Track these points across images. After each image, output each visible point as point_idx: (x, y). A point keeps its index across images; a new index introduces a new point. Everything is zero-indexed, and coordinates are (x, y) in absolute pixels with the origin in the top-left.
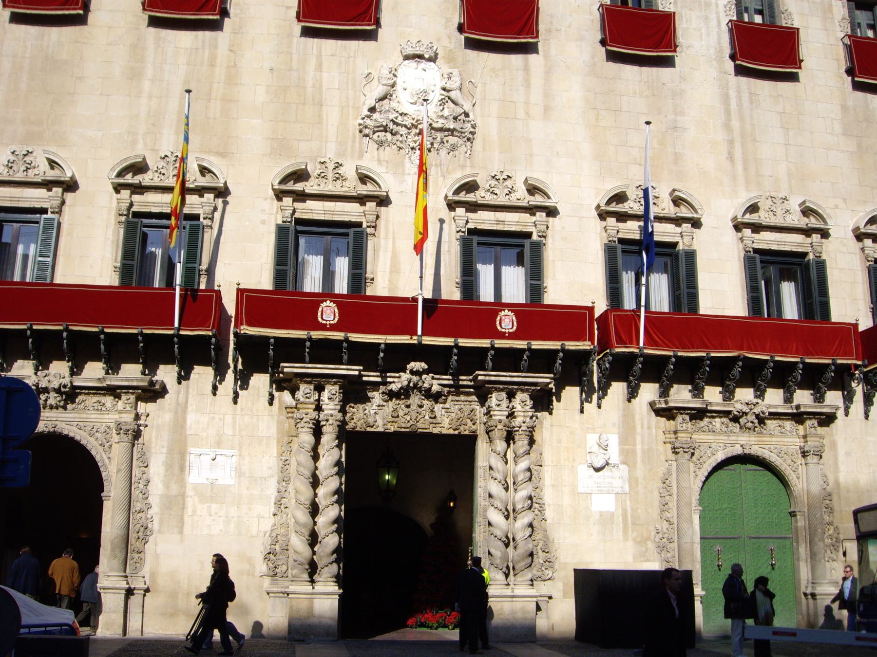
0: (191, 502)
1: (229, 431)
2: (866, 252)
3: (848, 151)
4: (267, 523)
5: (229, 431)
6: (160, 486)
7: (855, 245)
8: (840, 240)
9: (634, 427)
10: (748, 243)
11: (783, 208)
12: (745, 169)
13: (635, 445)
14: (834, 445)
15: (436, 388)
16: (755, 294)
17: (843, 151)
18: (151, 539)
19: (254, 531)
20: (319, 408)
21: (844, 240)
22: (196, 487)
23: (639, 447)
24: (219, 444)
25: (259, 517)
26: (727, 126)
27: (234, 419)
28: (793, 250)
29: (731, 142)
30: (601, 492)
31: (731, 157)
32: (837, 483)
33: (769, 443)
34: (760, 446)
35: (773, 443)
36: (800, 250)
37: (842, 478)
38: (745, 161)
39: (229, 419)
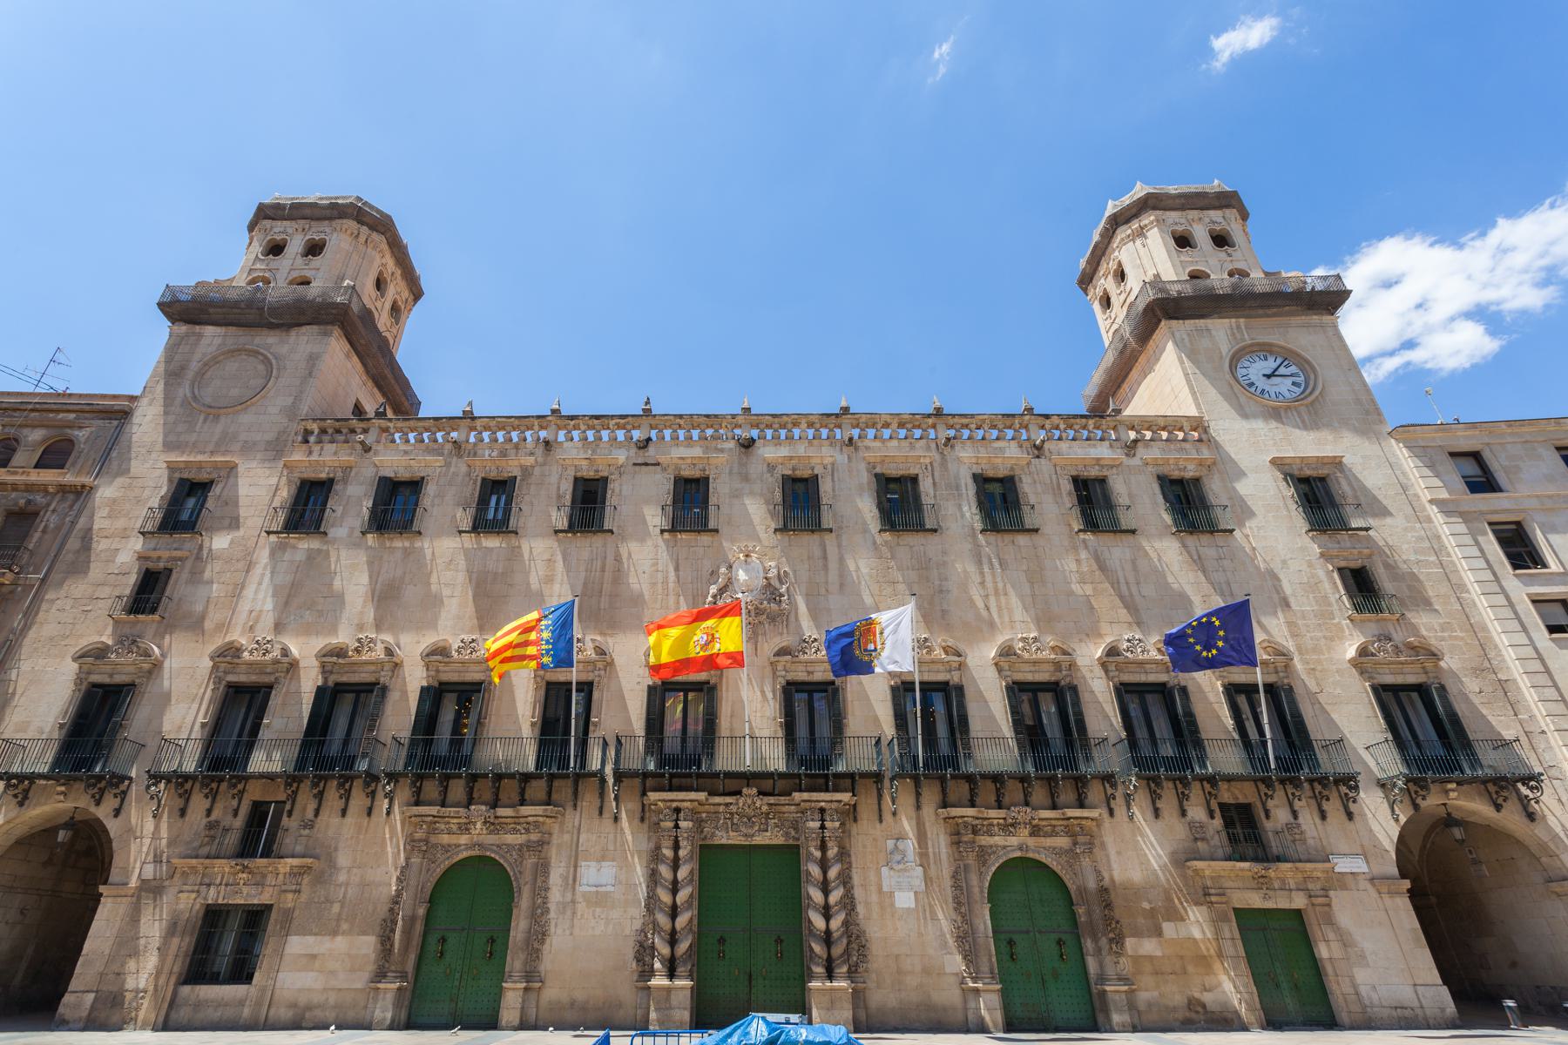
1: (611, 847)
4: (638, 925)
5: (611, 847)
6: (558, 894)
9: (925, 833)
13: (927, 849)
14: (1103, 846)
15: (765, 808)
18: (548, 941)
19: (627, 932)
20: (677, 826)
22: (584, 894)
23: (930, 850)
24: (603, 858)
25: (632, 918)
27: (616, 837)
32: (1112, 880)
39: (611, 836)
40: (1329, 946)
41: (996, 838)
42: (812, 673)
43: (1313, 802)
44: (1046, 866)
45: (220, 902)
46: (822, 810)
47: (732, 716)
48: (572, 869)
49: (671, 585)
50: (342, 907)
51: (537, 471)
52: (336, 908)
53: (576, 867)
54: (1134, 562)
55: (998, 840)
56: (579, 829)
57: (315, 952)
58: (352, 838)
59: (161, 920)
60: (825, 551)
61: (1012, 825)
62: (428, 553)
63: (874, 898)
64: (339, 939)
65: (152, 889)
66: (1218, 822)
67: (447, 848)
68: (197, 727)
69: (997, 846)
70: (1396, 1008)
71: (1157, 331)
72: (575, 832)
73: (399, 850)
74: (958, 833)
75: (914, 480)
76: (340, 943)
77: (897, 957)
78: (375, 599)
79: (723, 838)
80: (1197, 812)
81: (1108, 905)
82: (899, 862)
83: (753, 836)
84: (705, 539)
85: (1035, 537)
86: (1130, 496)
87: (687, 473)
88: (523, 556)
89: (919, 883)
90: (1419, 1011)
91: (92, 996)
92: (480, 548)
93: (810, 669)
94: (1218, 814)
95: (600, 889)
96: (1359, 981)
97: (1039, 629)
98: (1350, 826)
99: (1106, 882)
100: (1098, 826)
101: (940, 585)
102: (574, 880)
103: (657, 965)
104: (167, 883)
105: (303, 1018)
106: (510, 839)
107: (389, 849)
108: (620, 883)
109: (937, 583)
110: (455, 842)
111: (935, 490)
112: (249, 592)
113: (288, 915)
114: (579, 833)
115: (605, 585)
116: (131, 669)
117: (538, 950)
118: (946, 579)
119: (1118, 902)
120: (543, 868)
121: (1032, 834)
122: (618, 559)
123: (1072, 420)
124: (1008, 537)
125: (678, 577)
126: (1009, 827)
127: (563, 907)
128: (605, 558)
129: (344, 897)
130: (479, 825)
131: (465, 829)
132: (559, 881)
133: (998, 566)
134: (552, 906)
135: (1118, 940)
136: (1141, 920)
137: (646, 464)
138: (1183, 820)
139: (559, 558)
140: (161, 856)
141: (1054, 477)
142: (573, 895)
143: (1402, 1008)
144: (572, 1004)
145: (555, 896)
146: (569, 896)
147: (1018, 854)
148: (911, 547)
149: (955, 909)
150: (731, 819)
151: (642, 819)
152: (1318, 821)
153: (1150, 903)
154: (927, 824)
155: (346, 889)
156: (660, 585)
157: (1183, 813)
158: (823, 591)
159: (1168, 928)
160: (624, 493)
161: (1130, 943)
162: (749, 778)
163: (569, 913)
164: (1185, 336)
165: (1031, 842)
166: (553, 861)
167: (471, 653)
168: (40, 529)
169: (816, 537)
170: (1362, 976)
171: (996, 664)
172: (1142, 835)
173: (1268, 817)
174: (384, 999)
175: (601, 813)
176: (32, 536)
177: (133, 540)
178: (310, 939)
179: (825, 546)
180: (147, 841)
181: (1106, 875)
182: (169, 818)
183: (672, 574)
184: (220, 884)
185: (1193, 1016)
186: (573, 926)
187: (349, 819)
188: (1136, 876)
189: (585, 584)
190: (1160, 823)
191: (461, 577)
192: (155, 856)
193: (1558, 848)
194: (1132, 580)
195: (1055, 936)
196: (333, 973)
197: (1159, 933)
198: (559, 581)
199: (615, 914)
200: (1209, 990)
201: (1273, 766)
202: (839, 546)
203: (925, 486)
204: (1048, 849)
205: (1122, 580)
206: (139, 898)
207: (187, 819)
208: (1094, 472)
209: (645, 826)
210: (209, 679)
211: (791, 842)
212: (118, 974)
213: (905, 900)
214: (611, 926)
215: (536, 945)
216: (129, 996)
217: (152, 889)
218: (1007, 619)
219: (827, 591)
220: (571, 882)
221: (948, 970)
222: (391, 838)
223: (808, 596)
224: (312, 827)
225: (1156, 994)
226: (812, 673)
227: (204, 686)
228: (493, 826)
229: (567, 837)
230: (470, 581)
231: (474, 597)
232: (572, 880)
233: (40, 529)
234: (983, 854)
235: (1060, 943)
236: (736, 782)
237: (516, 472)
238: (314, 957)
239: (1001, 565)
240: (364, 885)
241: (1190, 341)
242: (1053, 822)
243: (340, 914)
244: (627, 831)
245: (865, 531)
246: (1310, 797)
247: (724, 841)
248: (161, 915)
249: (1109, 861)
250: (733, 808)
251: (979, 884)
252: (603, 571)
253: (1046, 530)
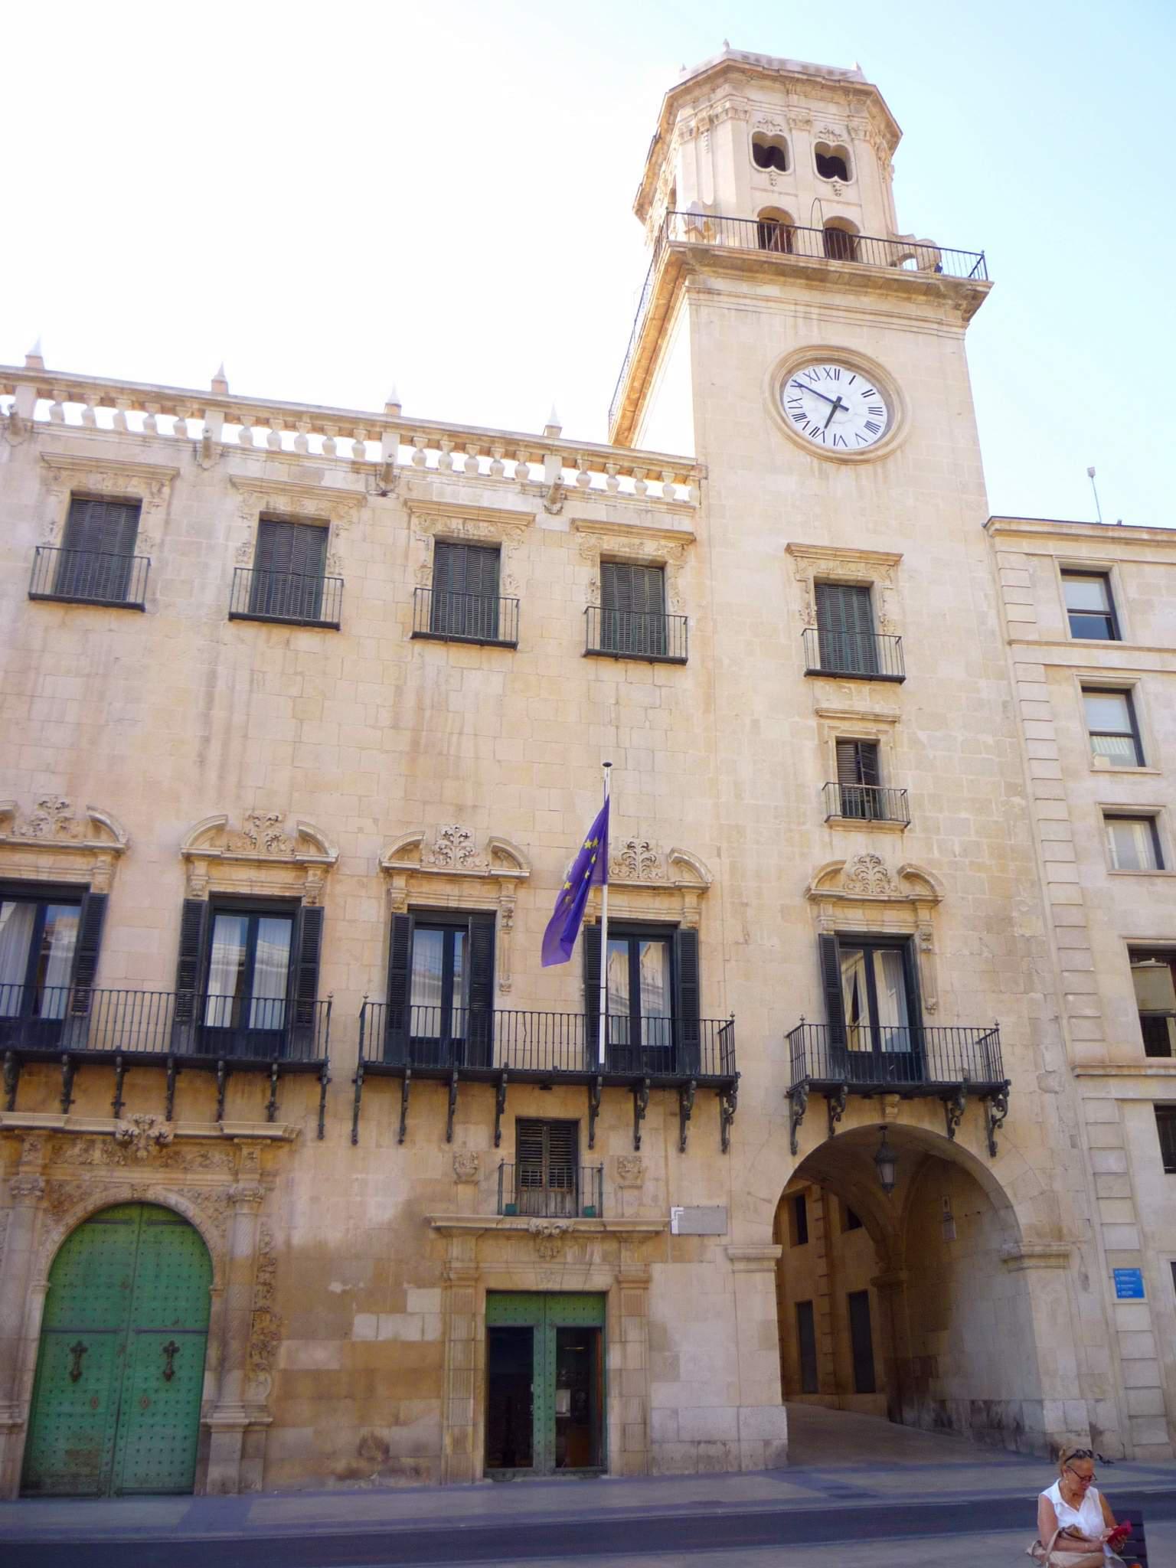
2: (393, 895)
3: (394, 751)
7: (377, 887)
8: (356, 878)
10: (198, 883)
11: (270, 832)
12: (221, 778)
14: (290, 1185)
16: (189, 959)
17: (387, 752)
21: (365, 880)
26: (206, 718)
28: (276, 894)
29: (206, 740)
31: (202, 760)
32: (288, 1243)
33: (181, 1182)
34: (165, 1186)
35: (188, 1183)
36: (287, 894)
38: (223, 767)
40: (624, 1351)
43: (676, 1121)
66: (507, 1151)
70: (699, 1443)
80: (474, 1136)
90: (733, 1447)
94: (509, 1133)
96: (655, 1403)
98: (722, 1161)
138: (446, 1147)
143: (709, 1442)
152: (672, 1151)
153: (344, 1282)
157: (449, 1138)
159: (365, 1326)
170: (662, 1395)
173: (591, 1147)
181: (279, 1238)
185: (363, 1464)
188: (334, 1235)
190: (402, 1150)
193: (1015, 1195)
197: (344, 1331)
200: (405, 1424)
201: (602, 1060)
225: (308, 1432)
235: (171, 1351)
246: (673, 1114)
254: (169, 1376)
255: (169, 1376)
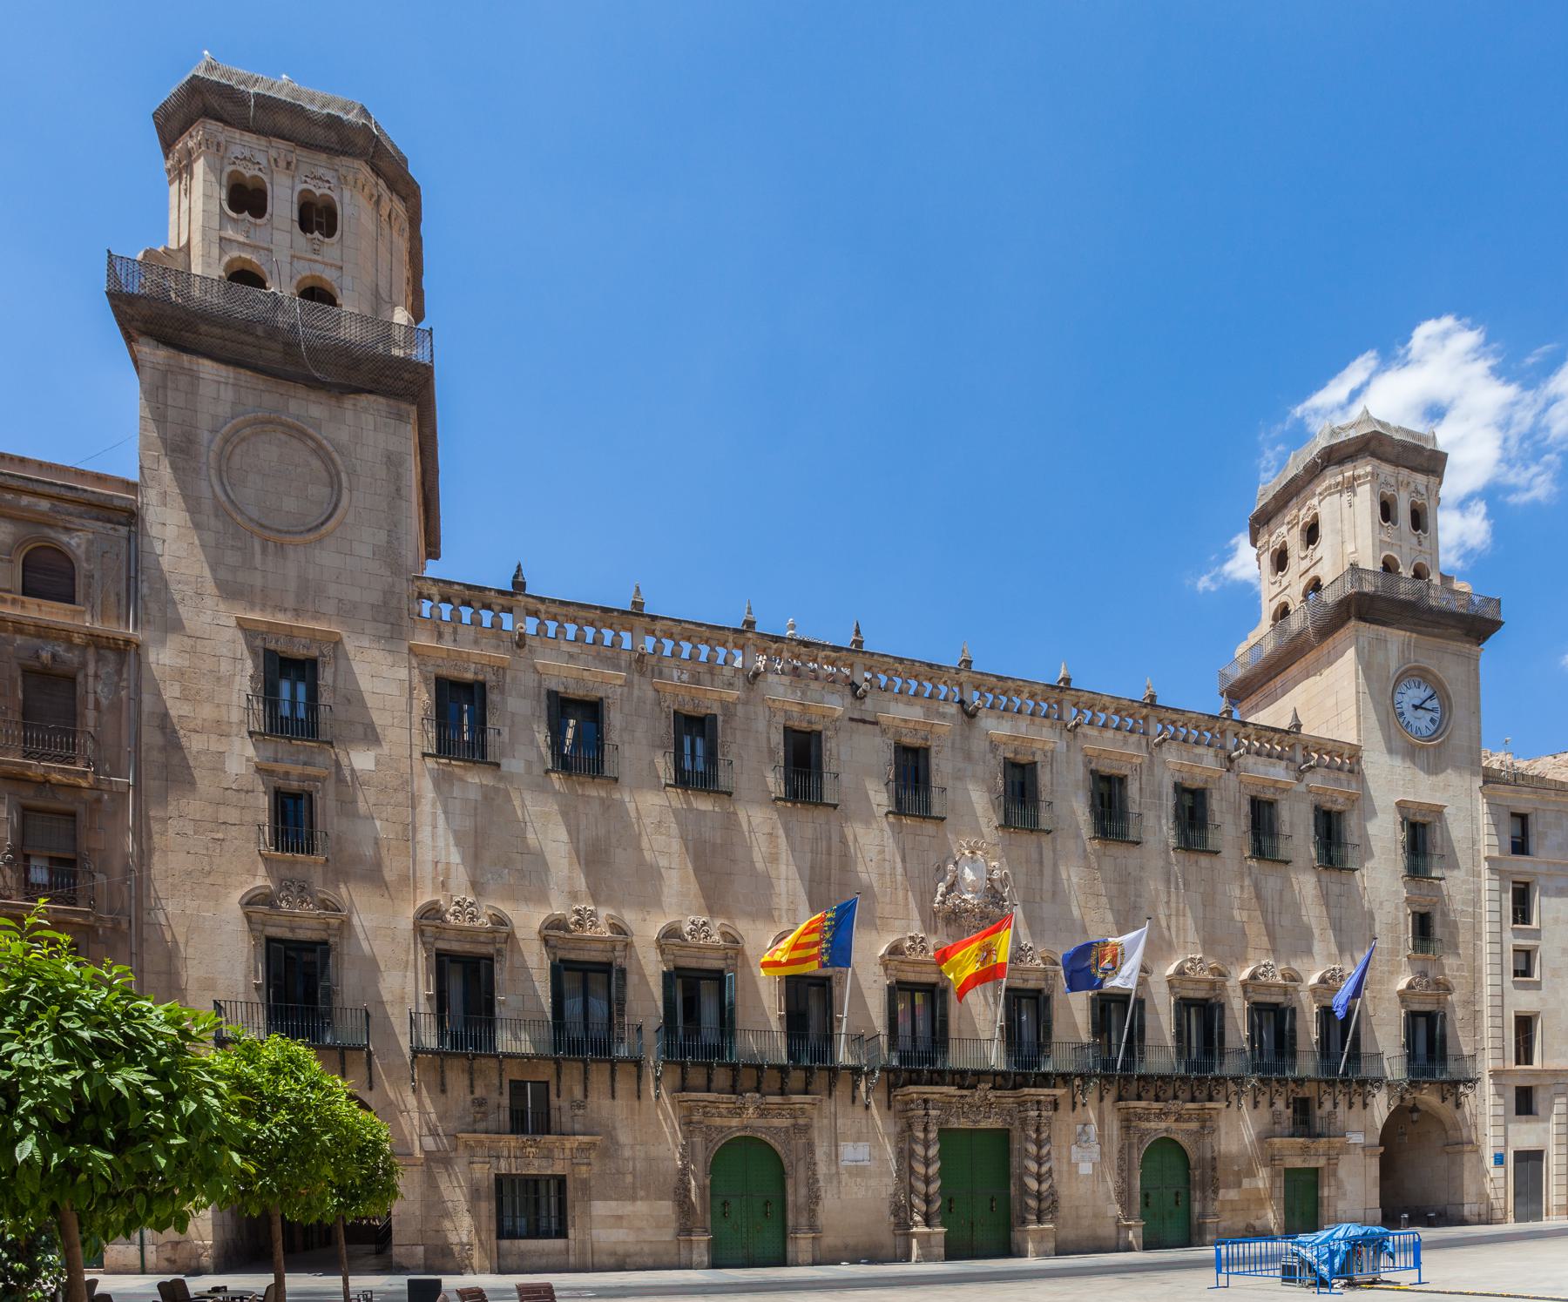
0: (845, 1177)
1: (865, 1130)
4: (891, 1190)
5: (865, 1130)
6: (824, 1168)
18: (821, 1203)
19: (883, 1196)
24: (858, 1139)
30: (1084, 1161)
32: (1219, 1151)
37: (1223, 1148)
39: (864, 1121)
41: (1152, 1123)
42: (1027, 980)
44: (1177, 1143)
45: (514, 1172)
46: (1039, 1102)
47: (959, 1018)
48: (833, 1148)
49: (899, 878)
50: (634, 1177)
51: (740, 710)
52: (629, 1179)
53: (836, 1146)
54: (1281, 892)
55: (1153, 1125)
56: (836, 1115)
57: (620, 1213)
58: (627, 1118)
59: (460, 1187)
60: (1041, 854)
61: (1164, 1114)
62: (631, 807)
63: (1065, 1167)
64: (639, 1203)
65: (437, 1161)
67: (720, 1129)
68: (422, 1000)
69: (1151, 1129)
71: (1342, 630)
72: (832, 1117)
73: (675, 1131)
74: (1128, 1120)
75: (1122, 780)
76: (641, 1207)
77: (1077, 1207)
78: (582, 862)
79: (955, 1123)
81: (1214, 1169)
82: (1086, 1142)
83: (979, 1121)
84: (929, 827)
85: (1214, 859)
86: (1292, 825)
87: (908, 740)
88: (741, 826)
89: (1096, 1156)
91: (422, 1247)
92: (691, 809)
93: (1025, 977)
95: (858, 1163)
97: (1204, 952)
99: (1216, 1154)
100: (1218, 1114)
101: (1135, 901)
102: (837, 1156)
103: (917, 1218)
104: (452, 1155)
105: (625, 1263)
106: (777, 1122)
107: (666, 1129)
108: (875, 1158)
109: (1133, 899)
110: (727, 1124)
111: (1141, 798)
112: (424, 834)
113: (585, 1185)
114: (836, 1119)
115: (833, 871)
116: (314, 923)
117: (814, 1210)
118: (1140, 896)
119: (1220, 1166)
120: (810, 1148)
121: (1176, 1120)
122: (843, 841)
123: (1263, 732)
124: (1193, 857)
125: (905, 869)
126: (1162, 1115)
127: (829, 1178)
128: (830, 838)
129: (634, 1169)
130: (751, 1110)
131: (738, 1111)
132: (824, 1158)
133: (1182, 887)
134: (821, 1177)
135: (1216, 1192)
136: (1231, 1178)
137: (864, 721)
139: (781, 832)
140: (437, 1130)
141: (1237, 794)
142: (837, 1167)
144: (846, 1247)
145: (822, 1169)
146: (833, 1170)
147: (1164, 1135)
148: (1115, 859)
149: (1118, 1174)
150: (963, 1108)
151: (889, 1107)
154: (1106, 1113)
155: (634, 1163)
156: (888, 876)
158: (1038, 899)
159: (1246, 1183)
160: (843, 757)
161: (1222, 1192)
162: (980, 1075)
163: (835, 1182)
164: (1366, 645)
165: (1174, 1126)
166: (816, 1141)
167: (706, 937)
168: (91, 705)
169: (1034, 837)
171: (1169, 981)
172: (1244, 1121)
174: (698, 1247)
175: (853, 1102)
176: (84, 716)
177: (237, 742)
178: (613, 1204)
179: (1041, 848)
180: (415, 1115)
181: (1216, 1148)
182: (428, 1092)
183: (899, 865)
184: (509, 1157)
186: (839, 1192)
187: (619, 1102)
189: (812, 868)
191: (676, 845)
192: (429, 1129)
194: (1277, 911)
195: (1174, 1190)
196: (640, 1229)
197: (1239, 1185)
198: (785, 862)
199: (873, 1183)
202: (1054, 850)
203: (1133, 789)
204: (1181, 1131)
205: (1270, 910)
206: (429, 1168)
207: (449, 1094)
208: (1268, 795)
209: (892, 1113)
210: (415, 944)
211: (1007, 1127)
212: (438, 1231)
213: (1085, 1169)
214: (870, 1192)
215: (812, 1207)
216: (456, 1249)
217: (437, 1161)
218: (1182, 940)
219: (1041, 898)
220: (833, 1158)
221: (1109, 1214)
222: (665, 1120)
223: (1025, 902)
224: (584, 1107)
226: (1027, 980)
227: (412, 952)
228: (763, 1112)
229: (826, 1121)
230: (687, 850)
231: (696, 870)
232: (835, 1157)
233: (91, 705)
234: (1143, 1134)
236: (966, 1079)
237: (716, 709)
238: (620, 1217)
239: (1184, 885)
240: (649, 1159)
241: (1369, 651)
242: (1191, 1112)
243: (634, 1184)
244: (877, 1117)
245: (1078, 836)
247: (956, 1126)
248: (459, 1182)
249: (1219, 1139)
250: (968, 1100)
251: (1137, 1156)
252: (829, 854)
253: (1225, 853)
254: (1177, 1203)
255: (1177, 1203)
